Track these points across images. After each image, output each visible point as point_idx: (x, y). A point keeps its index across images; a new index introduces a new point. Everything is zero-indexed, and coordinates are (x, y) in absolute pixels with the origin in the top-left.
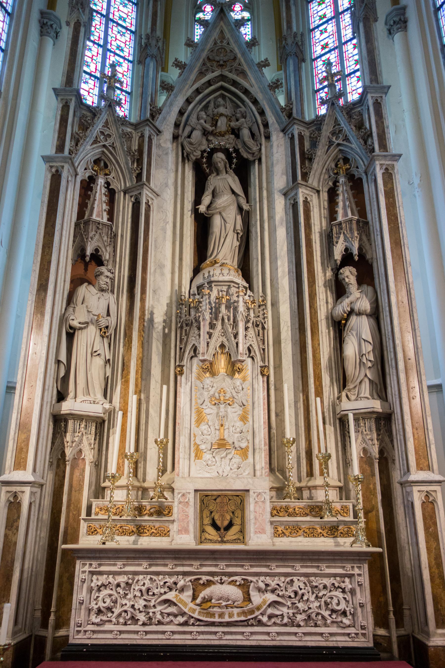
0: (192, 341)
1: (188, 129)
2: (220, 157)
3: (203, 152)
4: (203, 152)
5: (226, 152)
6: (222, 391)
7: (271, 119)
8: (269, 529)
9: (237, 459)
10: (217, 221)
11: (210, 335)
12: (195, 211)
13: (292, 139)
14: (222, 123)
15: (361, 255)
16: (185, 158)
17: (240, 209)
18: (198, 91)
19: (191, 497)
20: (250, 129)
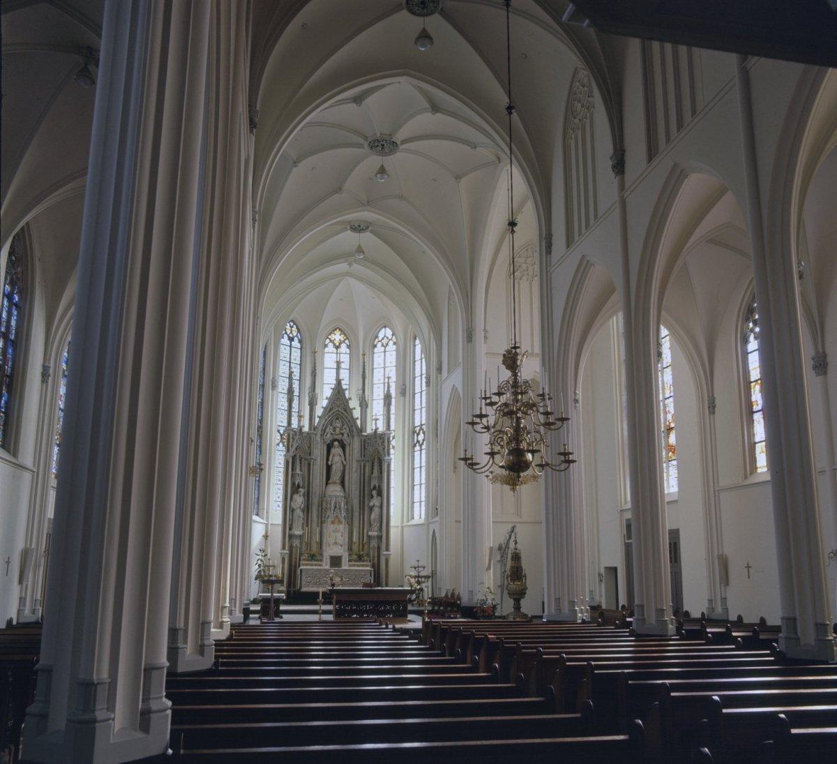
2: (336, 443)
5: (336, 440)
7: (355, 431)
9: (340, 547)
10: (334, 467)
12: (327, 463)
14: (338, 430)
15: (379, 486)
16: (324, 442)
17: (342, 462)
19: (329, 558)
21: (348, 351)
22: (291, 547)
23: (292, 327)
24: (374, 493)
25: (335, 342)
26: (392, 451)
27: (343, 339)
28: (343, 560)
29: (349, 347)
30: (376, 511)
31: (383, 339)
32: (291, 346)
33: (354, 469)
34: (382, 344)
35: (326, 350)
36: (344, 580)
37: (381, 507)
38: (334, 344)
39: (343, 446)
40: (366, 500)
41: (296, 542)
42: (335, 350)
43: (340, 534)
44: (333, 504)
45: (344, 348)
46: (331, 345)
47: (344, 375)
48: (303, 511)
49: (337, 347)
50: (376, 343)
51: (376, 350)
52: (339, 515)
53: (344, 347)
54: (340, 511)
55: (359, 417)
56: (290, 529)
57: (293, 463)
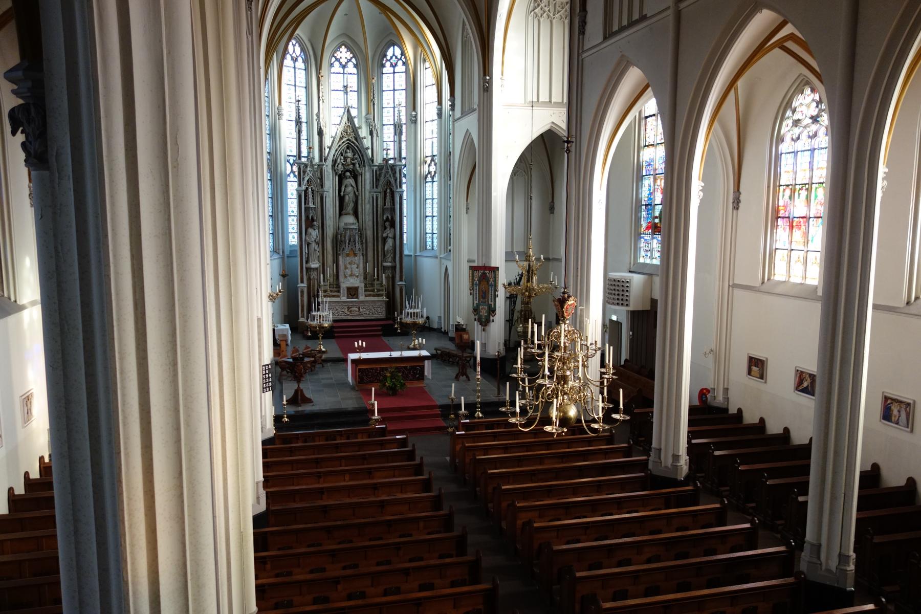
0: (343, 246)
1: (337, 164)
2: (348, 174)
3: (342, 171)
4: (342, 171)
5: (348, 171)
6: (352, 261)
8: (364, 295)
9: (356, 278)
10: (347, 197)
11: (348, 247)
13: (373, 170)
14: (349, 160)
16: (336, 174)
18: (340, 146)
20: (359, 164)
21: (355, 71)
22: (309, 279)
23: (294, 45)
24: (387, 224)
25: (341, 60)
26: (404, 180)
27: (349, 58)
28: (360, 290)
29: (356, 66)
30: (390, 242)
31: (391, 58)
32: (295, 68)
33: (367, 201)
34: (391, 63)
35: (333, 70)
36: (361, 310)
37: (394, 238)
38: (341, 63)
39: (355, 176)
40: (379, 231)
41: (314, 275)
42: (341, 70)
43: (356, 266)
44: (347, 238)
45: (351, 68)
46: (337, 64)
47: (353, 100)
48: (317, 244)
49: (344, 67)
50: (384, 62)
51: (385, 70)
52: (354, 249)
53: (350, 65)
54: (355, 244)
55: (370, 147)
56: (307, 262)
57: (306, 196)
